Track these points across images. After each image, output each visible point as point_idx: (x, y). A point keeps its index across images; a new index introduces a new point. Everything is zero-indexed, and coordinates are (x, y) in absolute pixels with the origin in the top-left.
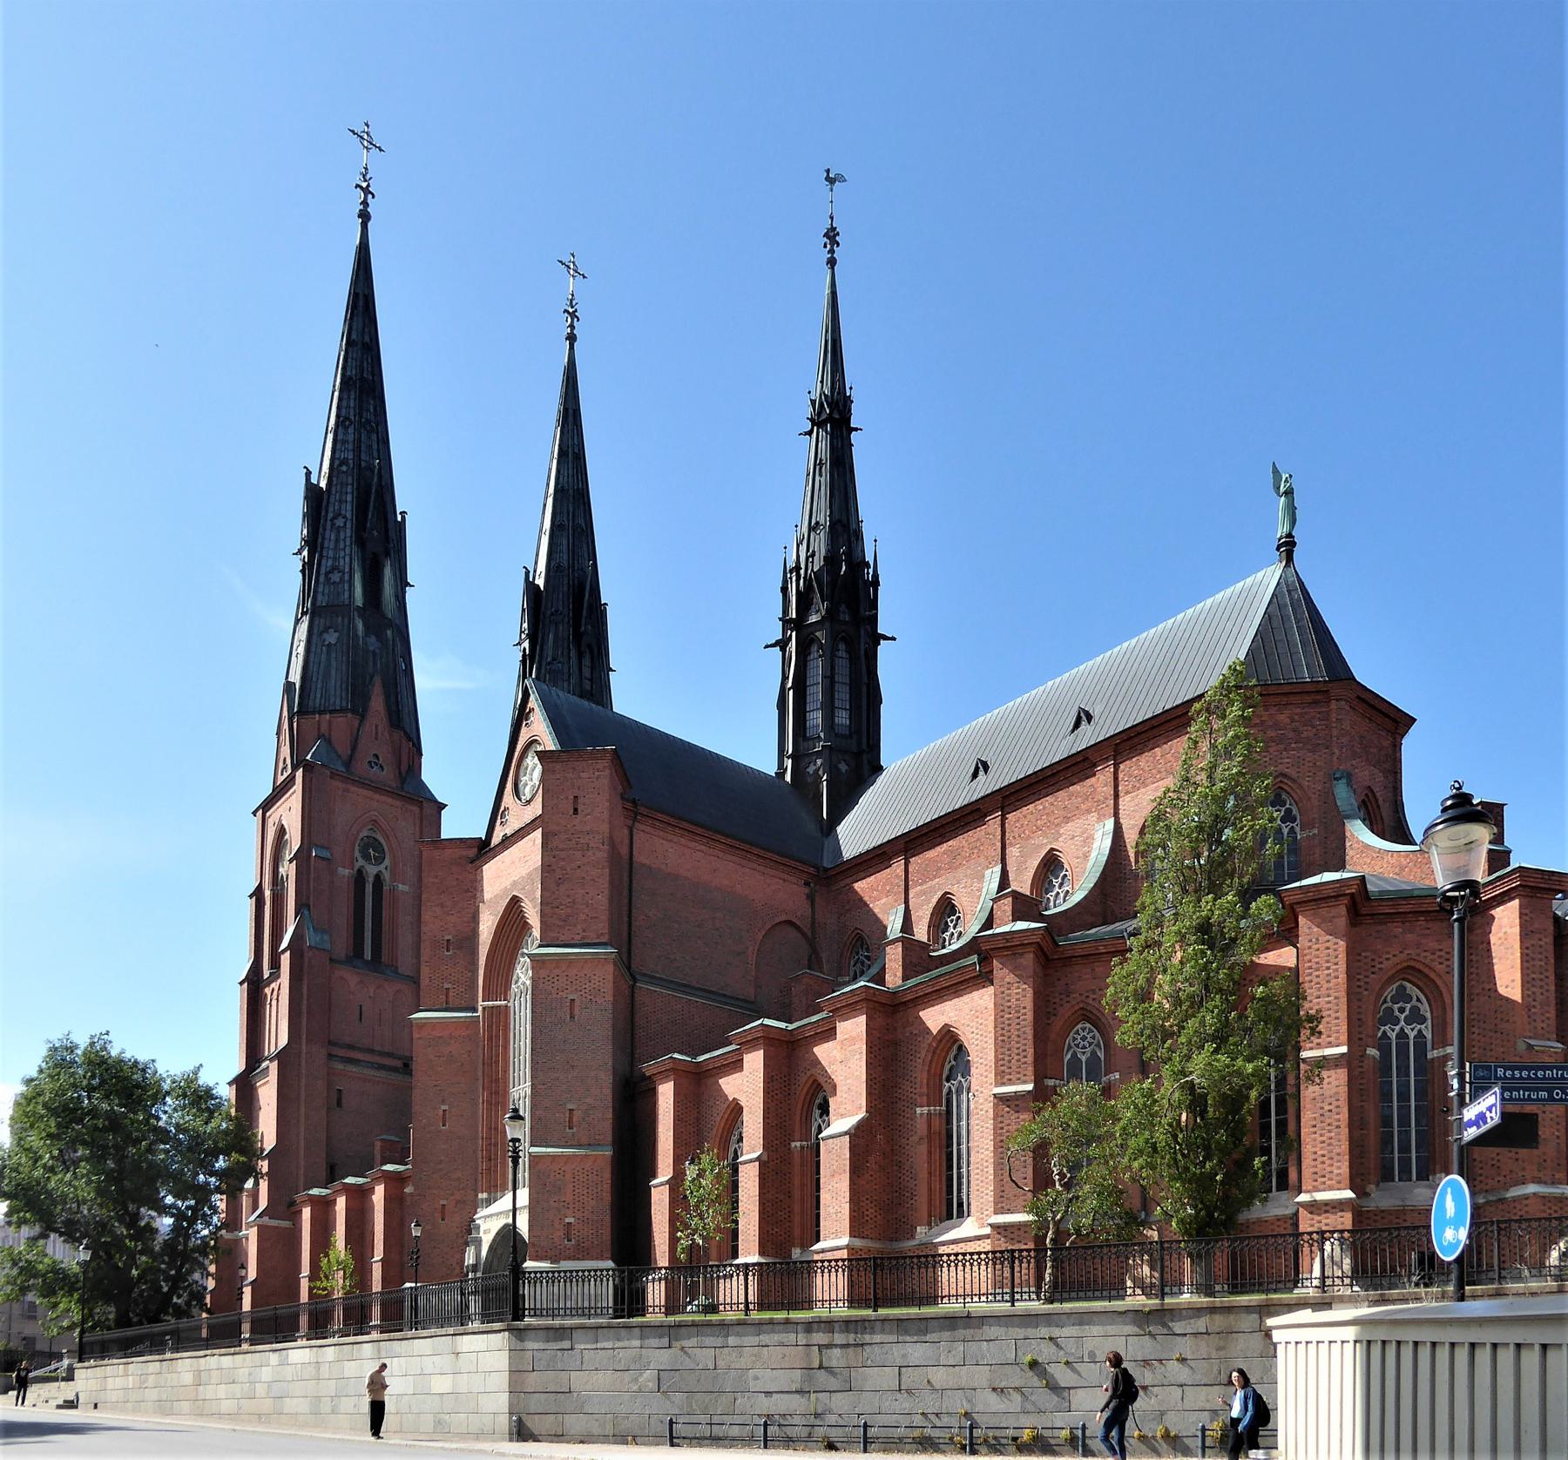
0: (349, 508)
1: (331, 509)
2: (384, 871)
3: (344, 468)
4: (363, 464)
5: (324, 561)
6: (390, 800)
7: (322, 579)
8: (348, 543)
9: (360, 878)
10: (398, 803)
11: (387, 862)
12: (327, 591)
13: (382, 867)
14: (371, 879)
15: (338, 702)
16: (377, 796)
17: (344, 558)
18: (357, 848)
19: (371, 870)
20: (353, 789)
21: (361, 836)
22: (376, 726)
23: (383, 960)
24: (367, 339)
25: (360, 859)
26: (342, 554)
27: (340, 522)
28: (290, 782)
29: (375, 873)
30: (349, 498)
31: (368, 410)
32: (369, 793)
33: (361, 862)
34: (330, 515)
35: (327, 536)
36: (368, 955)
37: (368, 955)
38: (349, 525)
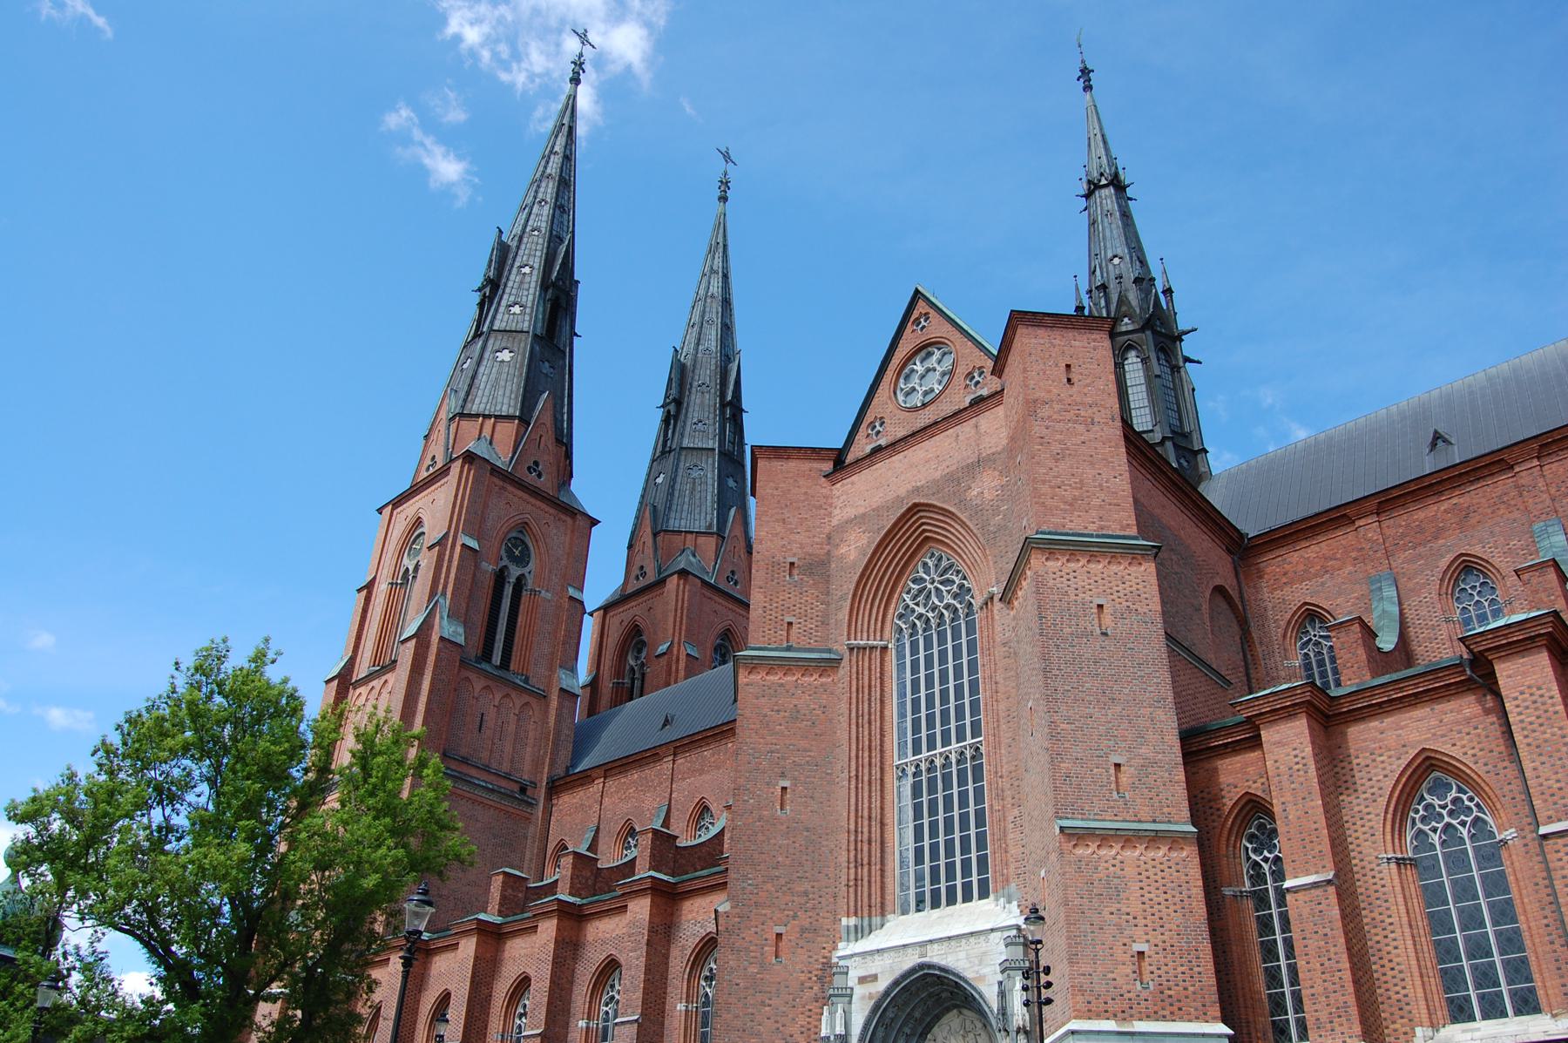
0: (537, 260)
1: (519, 259)
2: (527, 575)
3: (536, 233)
4: (554, 233)
5: (505, 297)
6: (543, 506)
7: (502, 309)
8: (533, 285)
9: (500, 577)
10: (552, 511)
11: (531, 566)
12: (505, 319)
13: (525, 571)
14: (513, 580)
15: (505, 408)
16: (533, 500)
17: (527, 296)
18: (504, 547)
19: (515, 571)
20: (510, 488)
21: (510, 536)
22: (541, 436)
23: (511, 668)
24: (568, 152)
25: (505, 558)
26: (525, 293)
27: (527, 270)
28: (444, 471)
29: (519, 573)
30: (538, 254)
31: (563, 198)
32: (526, 496)
33: (505, 562)
34: (517, 264)
35: (512, 277)
36: (497, 658)
37: (497, 658)
38: (535, 272)
